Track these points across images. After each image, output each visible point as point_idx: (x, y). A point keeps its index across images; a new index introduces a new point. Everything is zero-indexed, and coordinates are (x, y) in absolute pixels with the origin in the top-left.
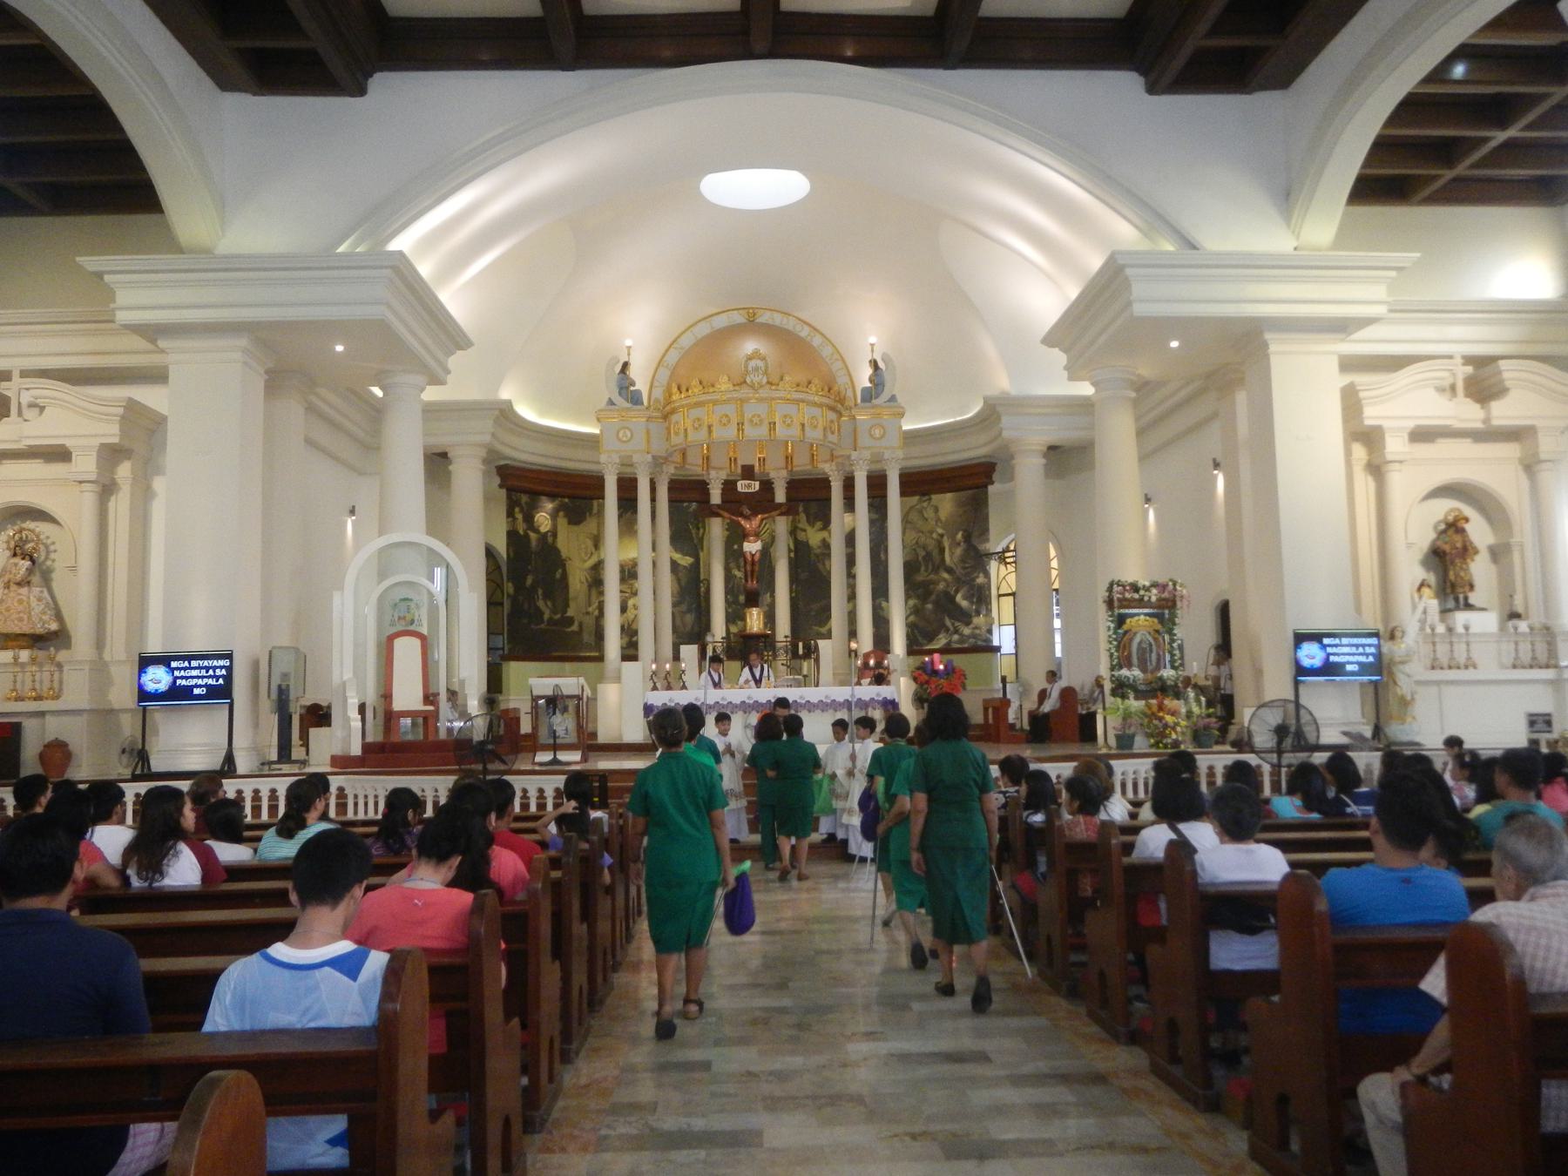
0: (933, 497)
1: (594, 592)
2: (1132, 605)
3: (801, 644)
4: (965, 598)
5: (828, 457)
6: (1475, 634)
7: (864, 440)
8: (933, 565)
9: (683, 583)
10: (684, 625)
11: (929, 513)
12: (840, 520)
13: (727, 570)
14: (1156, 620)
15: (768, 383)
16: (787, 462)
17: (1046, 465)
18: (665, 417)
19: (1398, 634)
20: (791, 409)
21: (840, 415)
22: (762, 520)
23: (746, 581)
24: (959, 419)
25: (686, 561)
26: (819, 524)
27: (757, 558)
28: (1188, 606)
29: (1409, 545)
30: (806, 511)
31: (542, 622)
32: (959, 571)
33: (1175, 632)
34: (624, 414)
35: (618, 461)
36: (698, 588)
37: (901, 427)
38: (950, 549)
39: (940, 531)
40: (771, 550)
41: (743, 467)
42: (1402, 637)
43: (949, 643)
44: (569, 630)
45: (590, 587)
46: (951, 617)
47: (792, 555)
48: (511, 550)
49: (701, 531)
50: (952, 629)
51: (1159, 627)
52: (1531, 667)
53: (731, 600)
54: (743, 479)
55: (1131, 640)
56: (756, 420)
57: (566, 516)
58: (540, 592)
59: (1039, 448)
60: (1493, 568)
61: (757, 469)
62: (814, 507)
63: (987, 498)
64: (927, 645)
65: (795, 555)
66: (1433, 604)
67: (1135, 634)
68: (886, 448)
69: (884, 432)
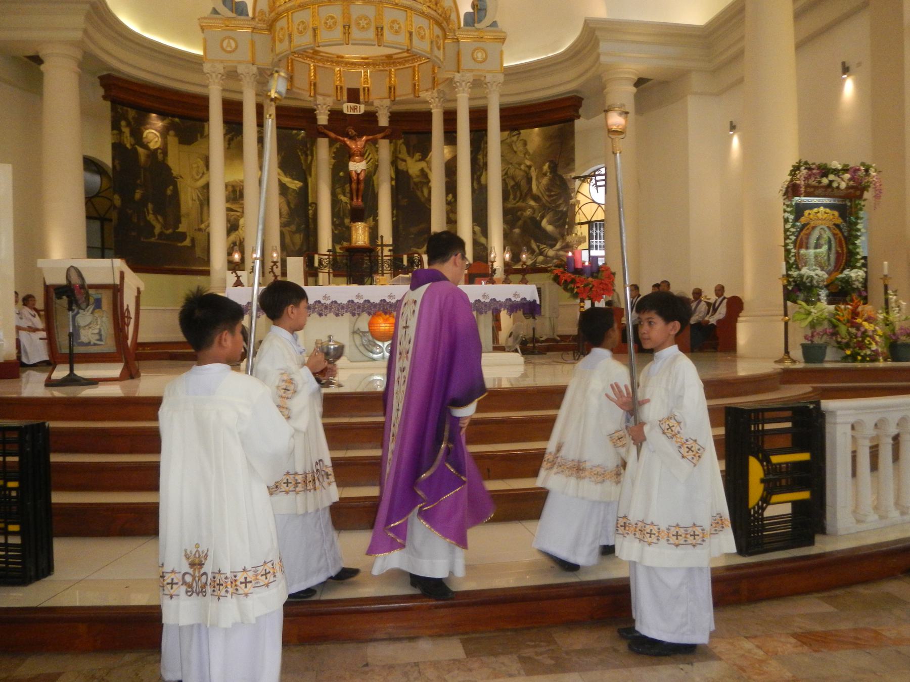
0: (522, 131)
1: (205, 208)
2: (817, 192)
3: (405, 258)
4: (550, 223)
5: (430, 86)
7: (466, 62)
8: (521, 195)
9: (292, 206)
10: (294, 244)
11: (518, 147)
12: (439, 152)
13: (334, 195)
14: (836, 213)
16: (390, 92)
17: (637, 97)
18: (271, 27)
20: (400, 15)
21: (445, 37)
22: (367, 141)
23: (352, 199)
24: (550, 55)
25: (294, 185)
26: (418, 156)
27: (362, 177)
28: (877, 197)
30: (407, 144)
31: (154, 237)
32: (545, 199)
33: (859, 227)
34: (227, 23)
35: (222, 71)
36: (307, 211)
38: (537, 179)
39: (528, 163)
40: (375, 178)
41: (349, 90)
43: (535, 263)
44: (179, 244)
45: (202, 205)
46: (536, 241)
47: (393, 183)
48: (117, 162)
49: (310, 158)
50: (537, 251)
51: (839, 221)
53: (337, 222)
54: (349, 102)
55: (808, 235)
56: (363, 23)
57: (176, 135)
58: (150, 206)
59: (633, 77)
61: (362, 98)
62: (414, 139)
63: (572, 133)
64: (515, 265)
65: (396, 183)
67: (814, 228)
69: (486, 56)
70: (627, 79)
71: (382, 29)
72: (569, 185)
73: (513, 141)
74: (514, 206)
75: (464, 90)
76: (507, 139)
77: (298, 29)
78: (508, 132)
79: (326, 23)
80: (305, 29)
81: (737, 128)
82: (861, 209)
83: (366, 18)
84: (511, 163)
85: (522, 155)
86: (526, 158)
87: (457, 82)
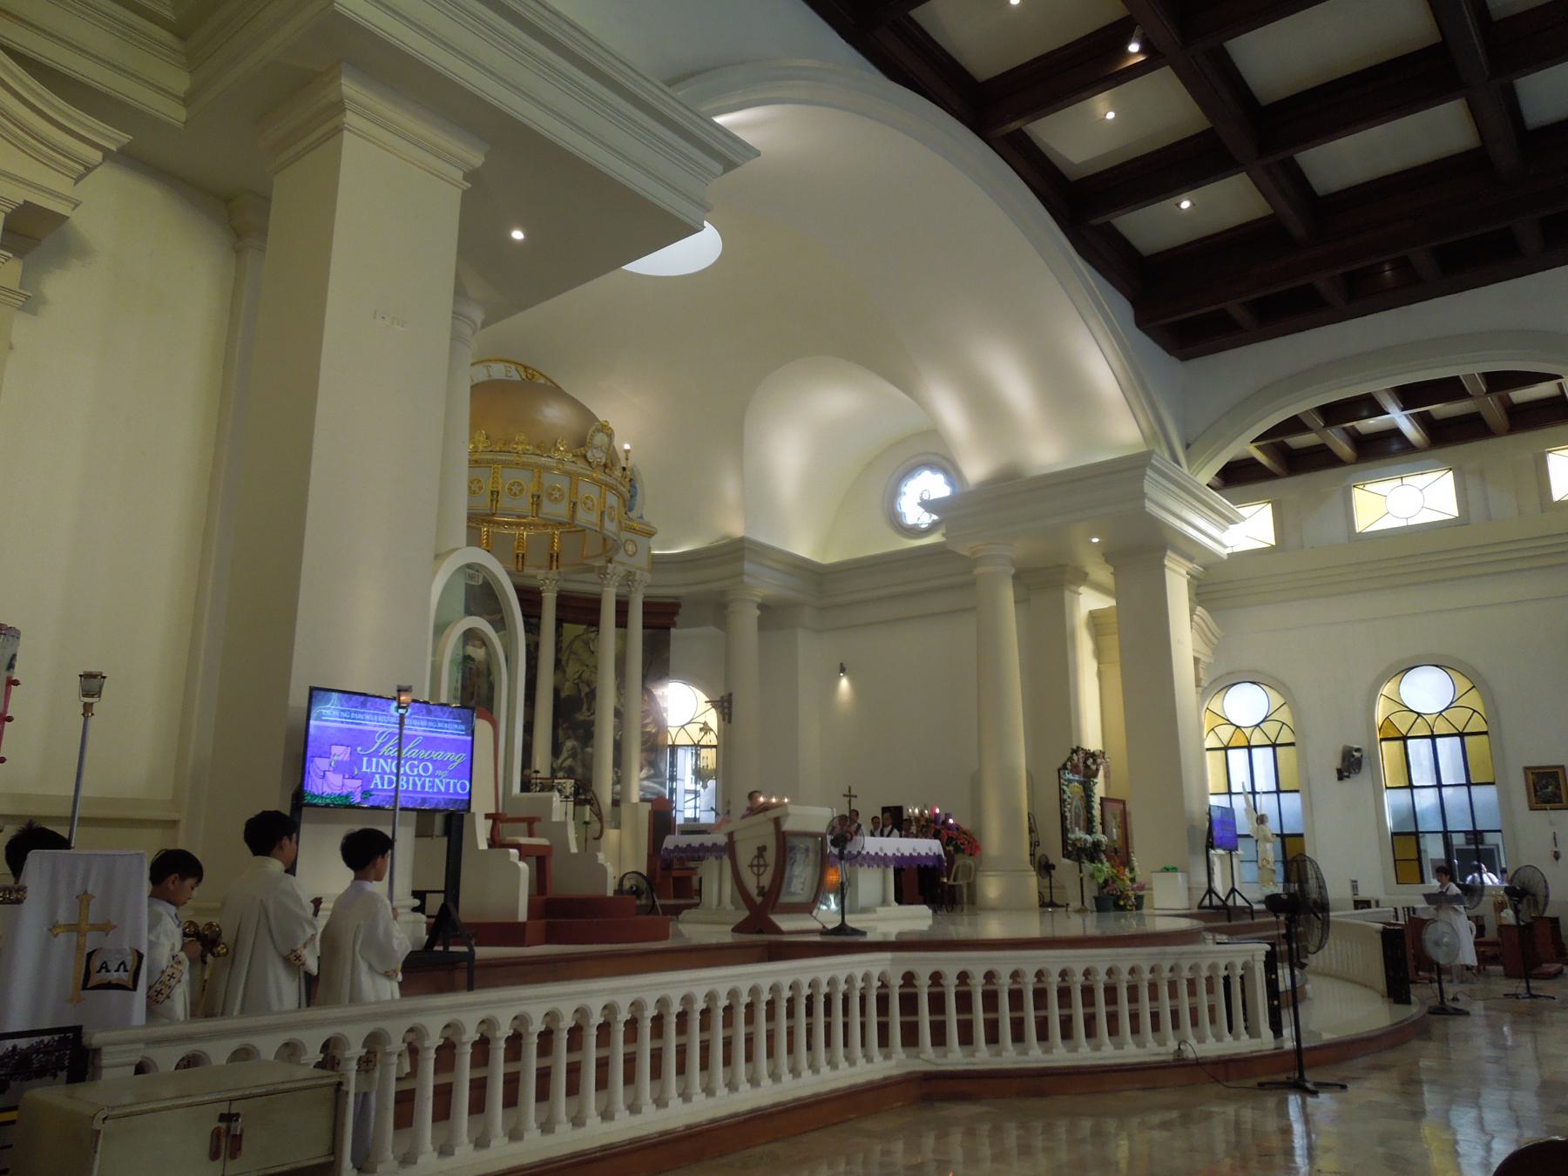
14: (1081, 787)
15: (605, 466)
17: (760, 619)
37: (650, 549)
51: (1083, 794)
56: (589, 504)
68: (638, 569)
69: (636, 550)
70: (756, 602)
71: (602, 513)
72: (661, 703)
73: (590, 639)
74: (587, 718)
75: (614, 584)
76: (583, 634)
77: (511, 490)
78: (585, 627)
79: (552, 494)
80: (521, 491)
81: (847, 671)
82: (1094, 785)
83: (592, 501)
84: (587, 666)
87: (608, 574)
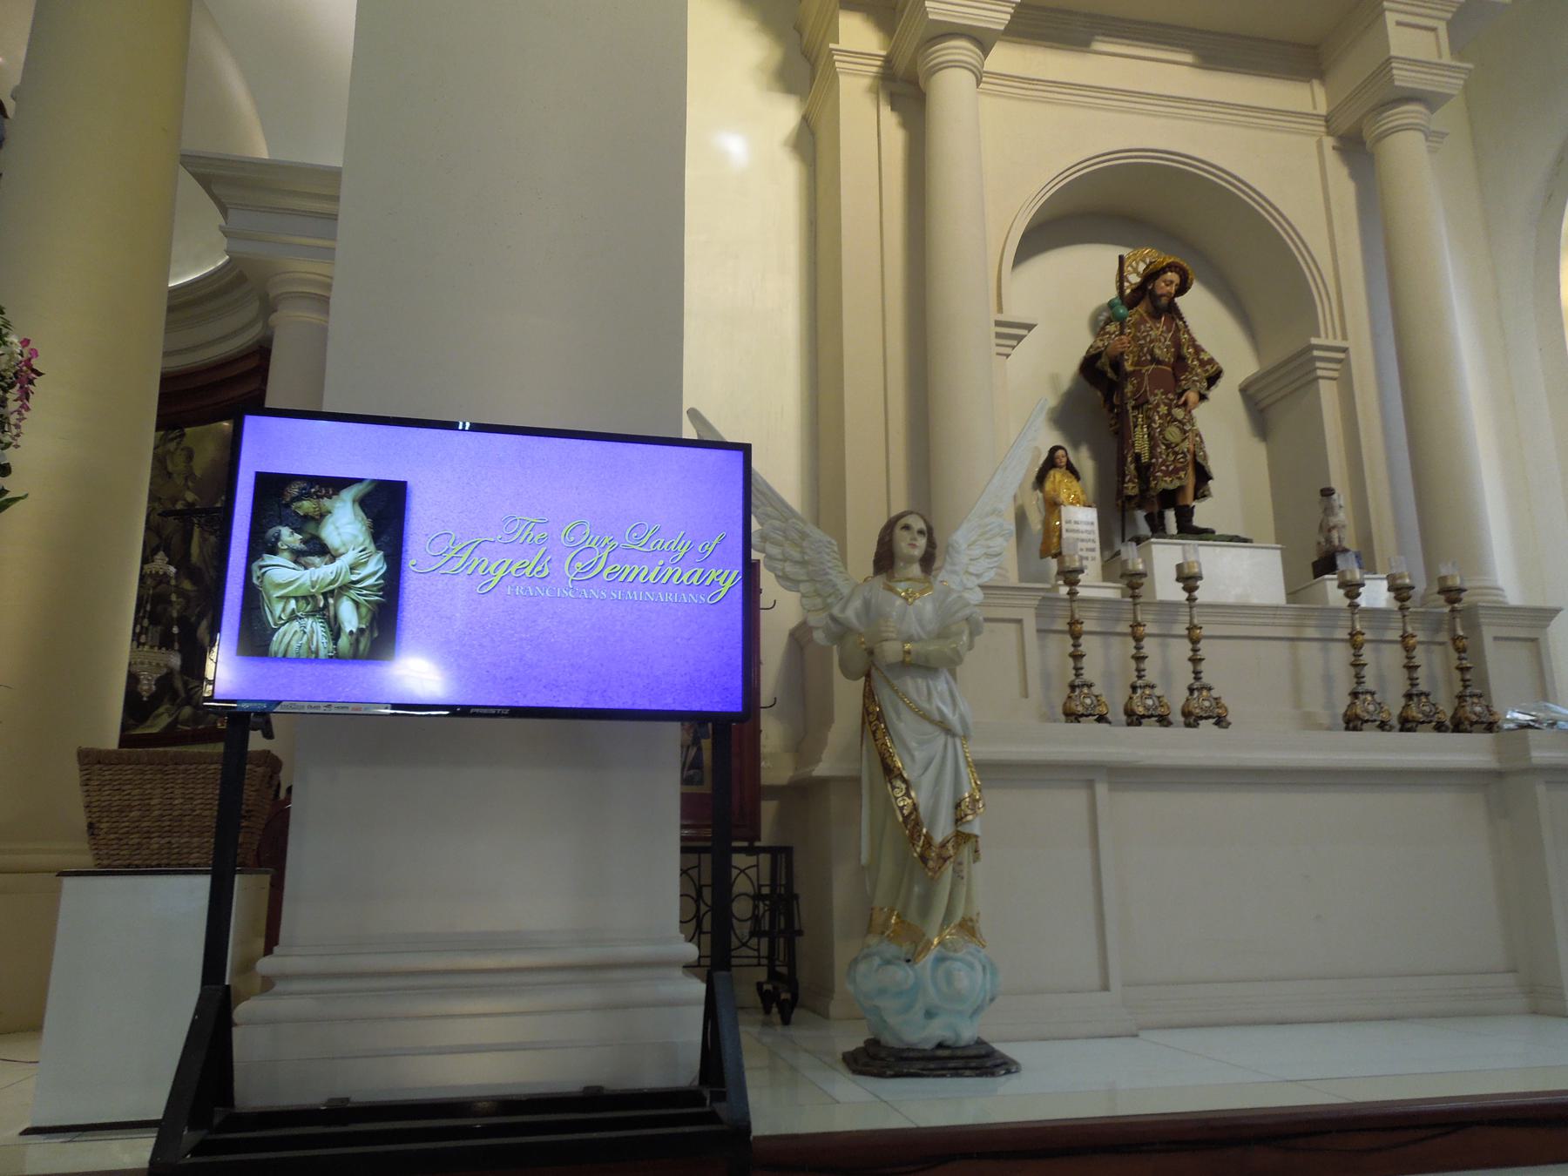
0: (187, 430)
6: (1220, 610)
11: (177, 465)
19: (910, 546)
29: (1012, 332)
42: (927, 561)
43: (175, 722)
50: (183, 695)
52: (1407, 724)
60: (1259, 451)
64: (137, 726)
66: (1081, 520)
78: (162, 433)
85: (180, 481)
86: (188, 488)
